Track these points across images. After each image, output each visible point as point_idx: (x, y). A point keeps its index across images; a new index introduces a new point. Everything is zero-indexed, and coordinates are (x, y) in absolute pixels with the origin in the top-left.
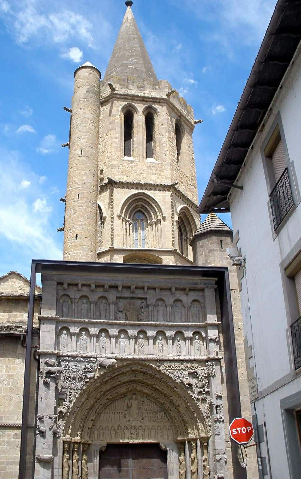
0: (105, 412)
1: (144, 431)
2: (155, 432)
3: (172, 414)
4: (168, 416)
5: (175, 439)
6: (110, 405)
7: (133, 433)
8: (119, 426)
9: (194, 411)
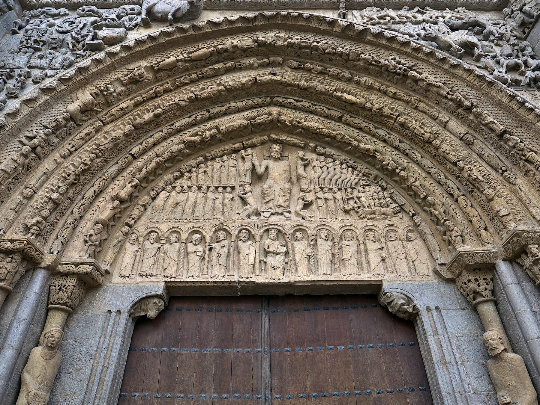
0: (174, 188)
1: (312, 243)
2: (358, 245)
3: (412, 180)
5: (441, 265)
6: (194, 169)
7: (272, 249)
8: (216, 231)
9: (505, 132)
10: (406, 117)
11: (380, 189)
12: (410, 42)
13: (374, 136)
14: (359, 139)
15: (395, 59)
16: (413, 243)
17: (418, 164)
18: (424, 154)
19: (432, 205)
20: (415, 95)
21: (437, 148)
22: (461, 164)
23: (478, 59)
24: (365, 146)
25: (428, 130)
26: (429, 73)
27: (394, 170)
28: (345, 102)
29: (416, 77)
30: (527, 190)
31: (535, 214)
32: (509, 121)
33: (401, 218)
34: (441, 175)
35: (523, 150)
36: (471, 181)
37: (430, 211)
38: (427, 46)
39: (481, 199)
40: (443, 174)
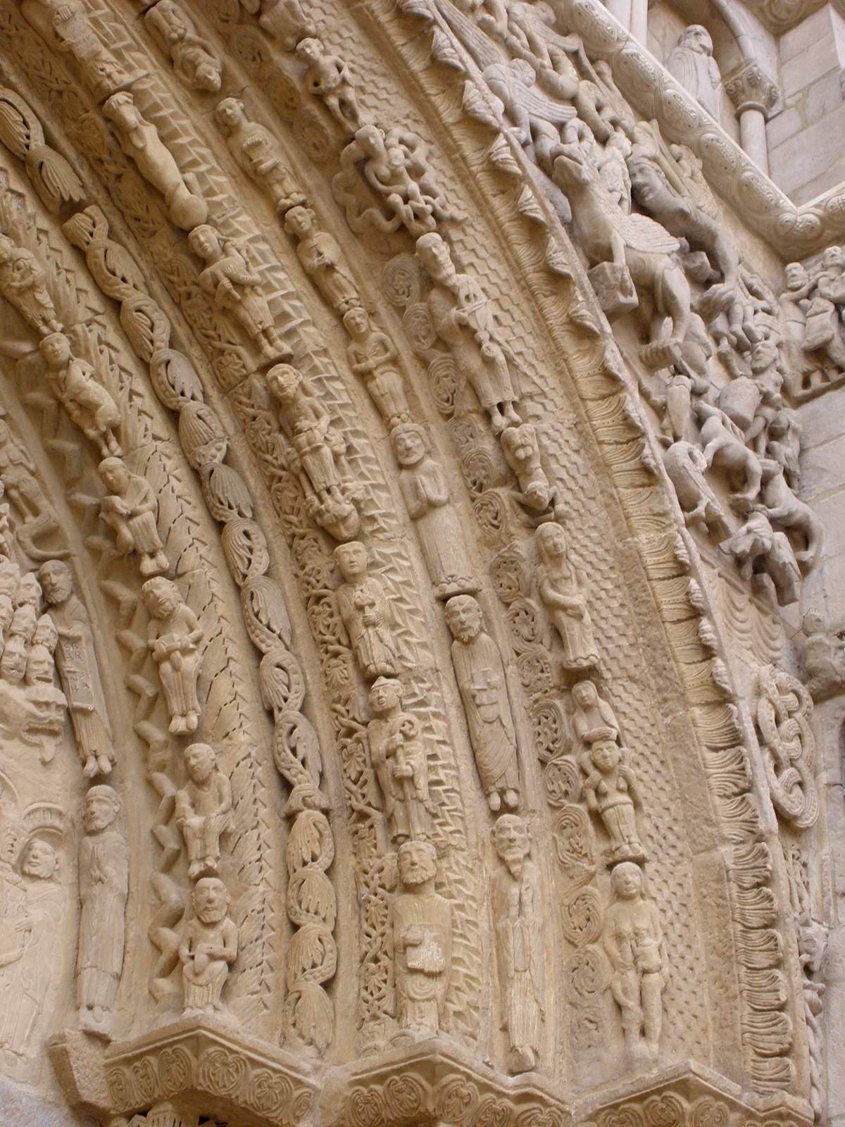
3: (177, 637)
4: (79, 665)
5: (92, 1037)
9: (591, 673)
10: (309, 382)
11: (35, 591)
12: (495, 133)
13: (146, 366)
14: (86, 339)
15: (412, 147)
16: (32, 887)
17: (240, 589)
18: (285, 569)
19: (195, 780)
20: (392, 330)
21: (346, 579)
22: (388, 690)
23: (657, 360)
24: (91, 384)
25: (356, 487)
26: (487, 286)
27: (135, 555)
28: (131, 160)
29: (439, 266)
30: (539, 920)
31: (515, 1022)
32: (624, 642)
33: (45, 763)
34: (294, 688)
35: (605, 772)
36: (385, 776)
37: (173, 804)
38: (540, 190)
39: (377, 863)
40: (302, 687)
